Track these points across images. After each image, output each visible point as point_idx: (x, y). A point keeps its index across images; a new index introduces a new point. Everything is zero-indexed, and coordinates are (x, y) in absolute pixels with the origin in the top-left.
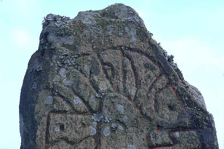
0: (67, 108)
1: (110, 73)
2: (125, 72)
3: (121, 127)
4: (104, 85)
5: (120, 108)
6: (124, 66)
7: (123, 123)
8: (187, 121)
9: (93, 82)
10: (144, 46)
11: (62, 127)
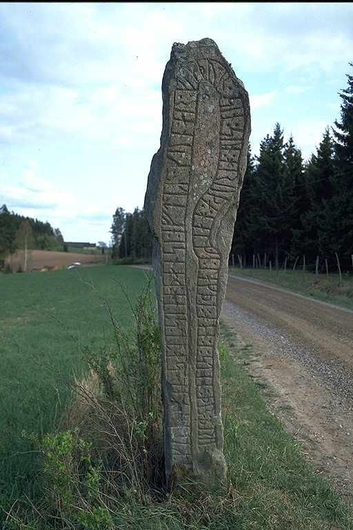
0: (184, 88)
1: (202, 71)
2: (209, 71)
3: (207, 97)
4: (200, 77)
5: (207, 88)
6: (209, 68)
7: (208, 95)
8: (237, 95)
9: (195, 75)
10: (218, 58)
11: (181, 97)
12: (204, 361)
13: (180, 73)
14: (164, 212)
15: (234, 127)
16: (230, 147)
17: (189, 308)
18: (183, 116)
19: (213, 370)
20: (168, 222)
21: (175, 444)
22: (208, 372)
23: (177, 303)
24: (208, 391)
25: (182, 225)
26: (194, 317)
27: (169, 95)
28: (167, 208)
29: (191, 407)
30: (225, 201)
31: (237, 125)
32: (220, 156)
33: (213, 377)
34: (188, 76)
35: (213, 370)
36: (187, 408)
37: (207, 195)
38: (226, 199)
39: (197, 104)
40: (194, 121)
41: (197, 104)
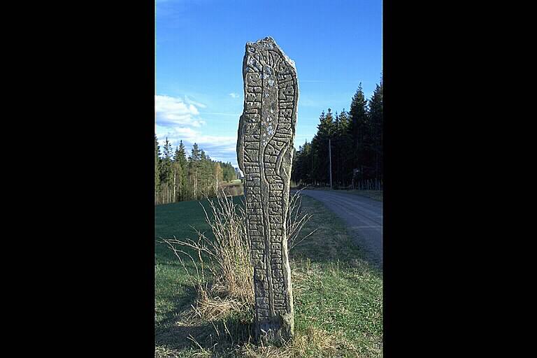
12: (276, 253)
13: (250, 62)
15: (287, 93)
17: (264, 217)
18: (254, 90)
22: (279, 260)
23: (257, 214)
25: (257, 162)
31: (289, 92)
33: (282, 264)
36: (266, 285)
38: (284, 142)
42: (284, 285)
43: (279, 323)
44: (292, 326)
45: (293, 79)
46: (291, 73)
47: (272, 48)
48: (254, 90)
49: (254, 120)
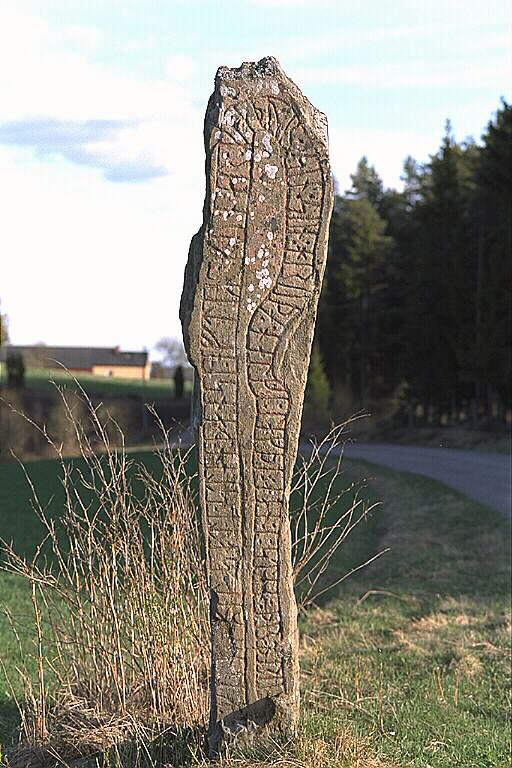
11: (228, 155)
13: (226, 120)
14: (204, 327)
15: (308, 198)
16: (302, 230)
17: (241, 474)
18: (232, 185)
19: (278, 569)
20: (211, 344)
21: (221, 686)
24: (271, 602)
26: (250, 487)
27: (212, 151)
28: (210, 323)
29: (246, 628)
30: (297, 311)
32: (287, 242)
34: (238, 123)
35: (278, 569)
36: (239, 632)
37: (269, 302)
39: (252, 165)
40: (248, 190)
41: (252, 165)
42: (281, 630)
43: (266, 711)
44: (295, 717)
45: (321, 168)
46: (317, 155)
47: (276, 91)
48: (232, 185)
49: (227, 252)
